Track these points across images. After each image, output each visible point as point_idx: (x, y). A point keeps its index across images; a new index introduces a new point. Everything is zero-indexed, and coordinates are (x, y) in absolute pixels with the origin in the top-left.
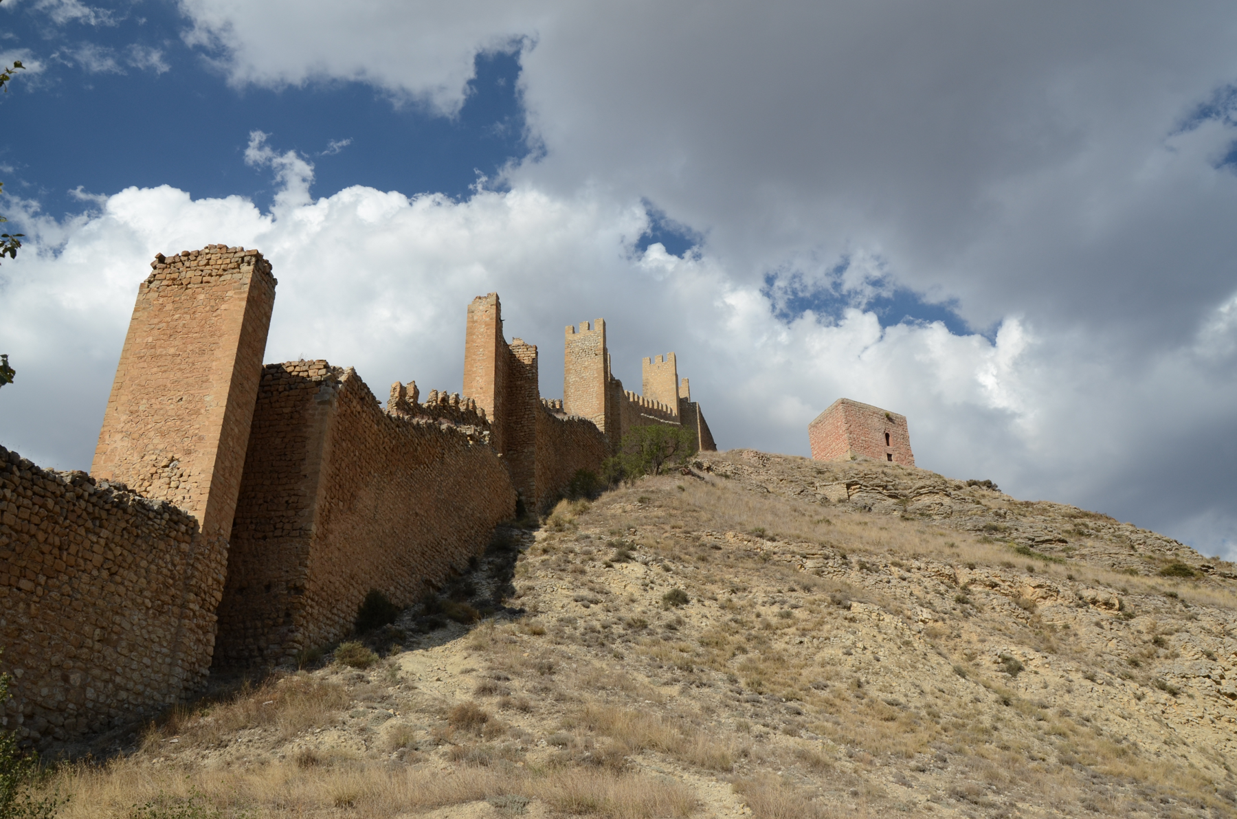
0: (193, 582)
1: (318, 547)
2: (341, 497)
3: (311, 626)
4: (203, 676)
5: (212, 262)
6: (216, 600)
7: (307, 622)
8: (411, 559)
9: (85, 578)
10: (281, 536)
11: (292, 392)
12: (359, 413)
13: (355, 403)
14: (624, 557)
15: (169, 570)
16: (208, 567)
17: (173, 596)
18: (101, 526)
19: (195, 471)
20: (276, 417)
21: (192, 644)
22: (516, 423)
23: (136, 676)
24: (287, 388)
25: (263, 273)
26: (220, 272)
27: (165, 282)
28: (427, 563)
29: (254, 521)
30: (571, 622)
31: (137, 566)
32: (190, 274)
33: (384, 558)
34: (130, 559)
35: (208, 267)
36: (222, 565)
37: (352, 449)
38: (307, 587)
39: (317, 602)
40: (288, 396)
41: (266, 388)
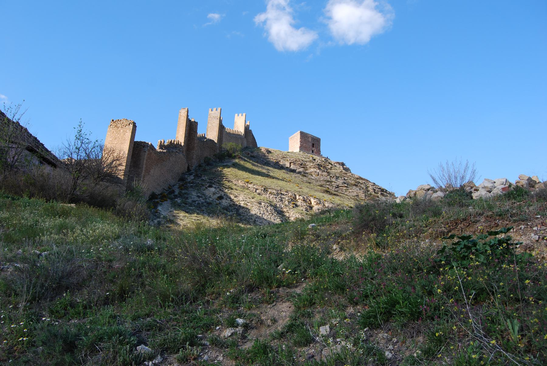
14: (210, 186)
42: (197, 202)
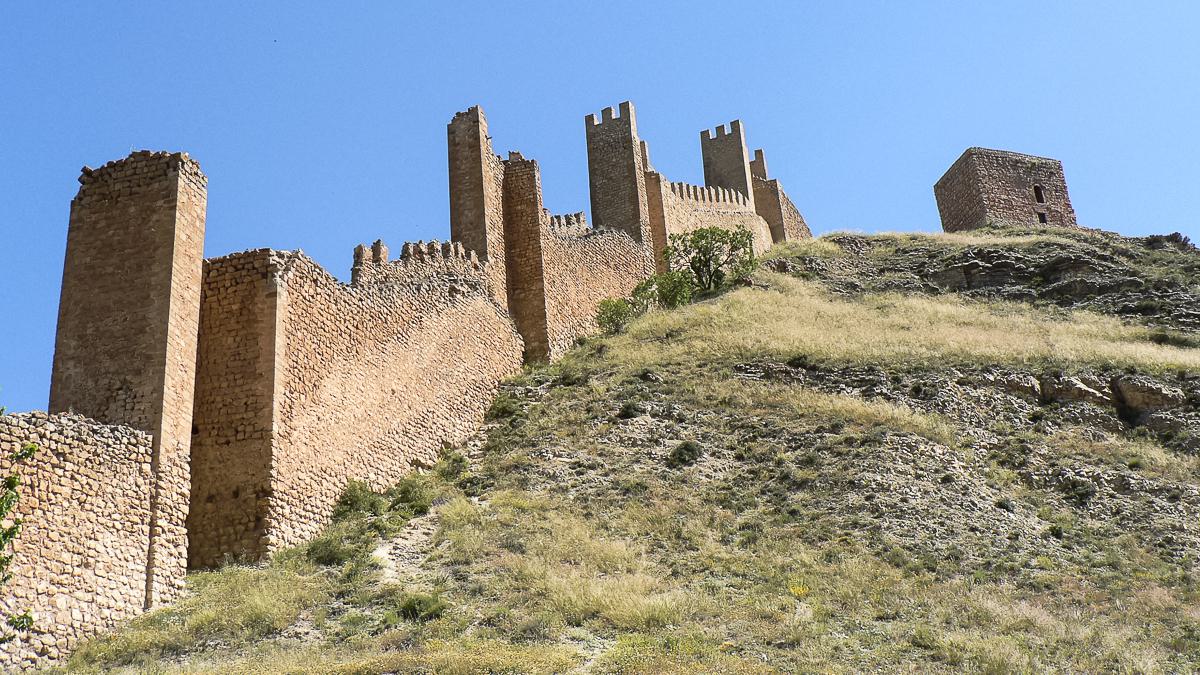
1: (282, 447)
3: (283, 526)
4: (179, 588)
9: (58, 510)
12: (313, 297)
22: (520, 256)
23: (116, 594)
24: (234, 284)
26: (148, 181)
27: (95, 198)
28: (412, 442)
29: (216, 426)
32: (118, 186)
33: (359, 445)
34: (95, 486)
36: (185, 479)
41: (212, 286)
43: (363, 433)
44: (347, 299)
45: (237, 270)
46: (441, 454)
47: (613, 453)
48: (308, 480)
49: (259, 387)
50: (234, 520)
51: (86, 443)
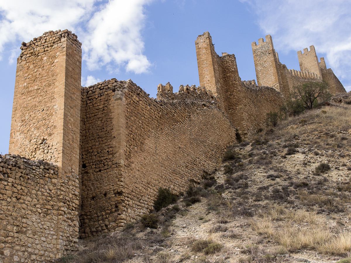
0: (61, 197)
1: (127, 171)
2: (135, 145)
3: (129, 210)
4: (75, 242)
5: (47, 40)
6: (76, 204)
7: (127, 209)
8: (180, 170)
10: (108, 169)
11: (102, 98)
12: (138, 101)
13: (135, 97)
14: (292, 152)
15: (48, 193)
16: (69, 189)
17: (52, 205)
18: (8, 177)
19: (54, 144)
20: (97, 111)
21: (66, 227)
22: (230, 95)
23: (39, 247)
24: (100, 96)
25: (73, 40)
26: (52, 44)
27: (28, 55)
28: (189, 171)
29: (94, 164)
30: (266, 188)
31: (31, 193)
32: (38, 48)
35: (46, 43)
36: (76, 187)
37: (137, 120)
38: (124, 191)
39: (131, 198)
40: (101, 99)
41: (90, 98)
42: (270, 189)
43: (167, 166)
44: (155, 104)
45: (101, 90)
46: (204, 177)
47: (287, 171)
48: (141, 188)
49: (114, 143)
50: (105, 208)
51: (19, 168)
